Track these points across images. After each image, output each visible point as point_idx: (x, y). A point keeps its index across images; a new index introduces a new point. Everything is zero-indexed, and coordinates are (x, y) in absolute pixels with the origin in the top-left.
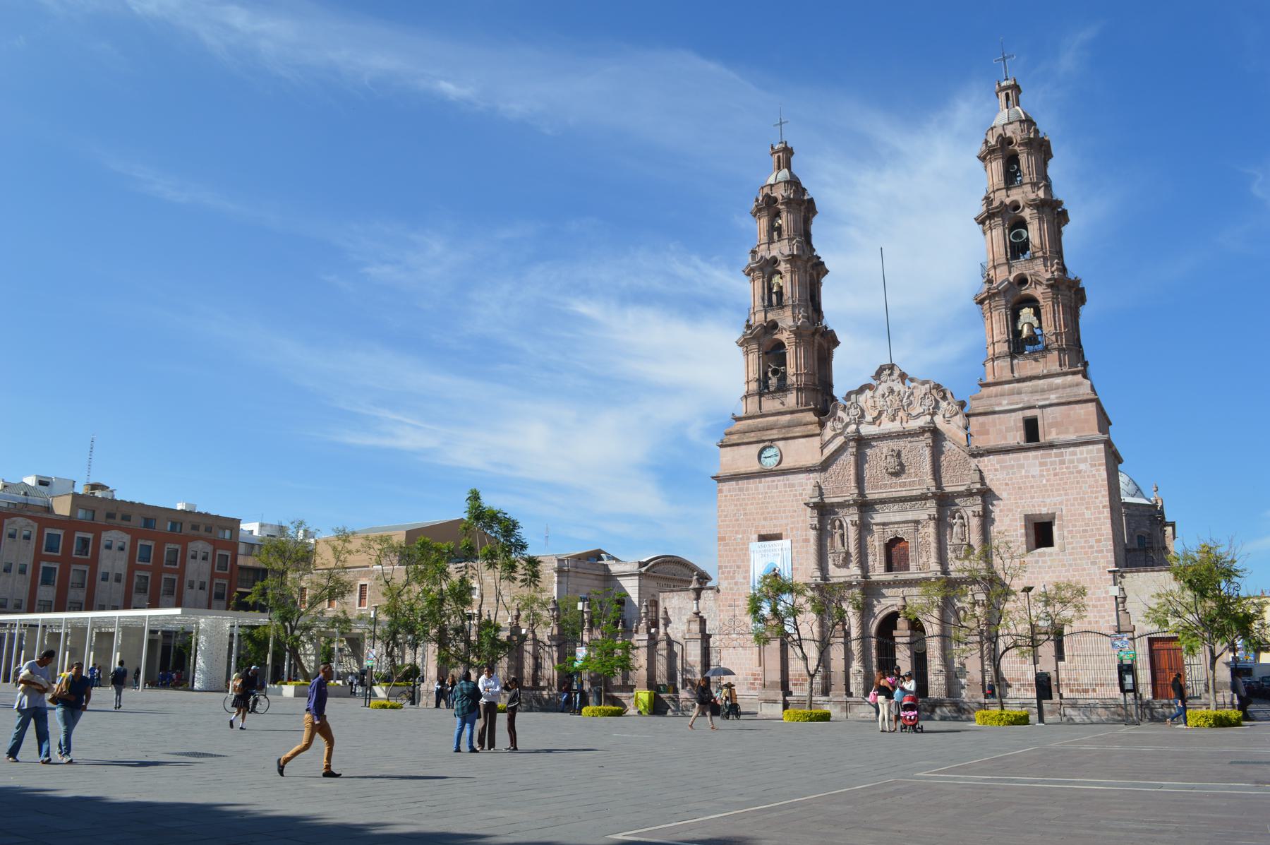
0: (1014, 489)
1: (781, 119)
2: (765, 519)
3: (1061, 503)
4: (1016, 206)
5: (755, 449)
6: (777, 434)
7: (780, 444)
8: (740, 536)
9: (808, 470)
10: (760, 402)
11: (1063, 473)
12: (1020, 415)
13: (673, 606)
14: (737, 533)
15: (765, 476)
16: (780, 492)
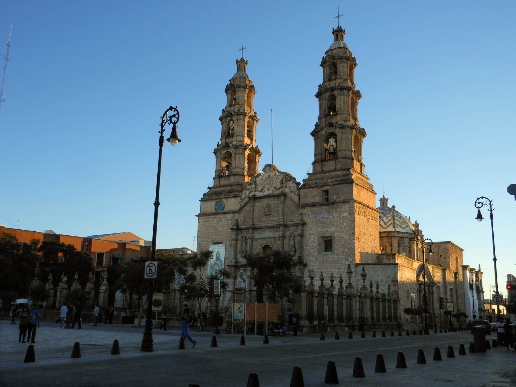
0: (316, 223)
1: (243, 47)
2: (216, 235)
3: (335, 231)
4: (332, 89)
5: (213, 203)
6: (224, 196)
7: (224, 200)
8: (206, 243)
9: (234, 212)
10: (219, 180)
11: (337, 217)
12: (321, 189)
14: (204, 241)
16: (223, 223)
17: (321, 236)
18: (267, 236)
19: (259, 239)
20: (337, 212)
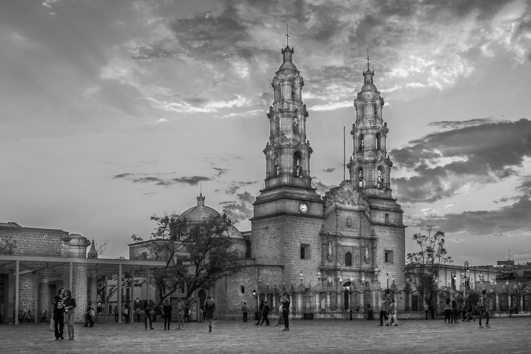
2: (303, 237)
8: (293, 243)
13: (263, 273)
14: (292, 241)
15: (304, 217)
17: (385, 250)
19: (342, 246)
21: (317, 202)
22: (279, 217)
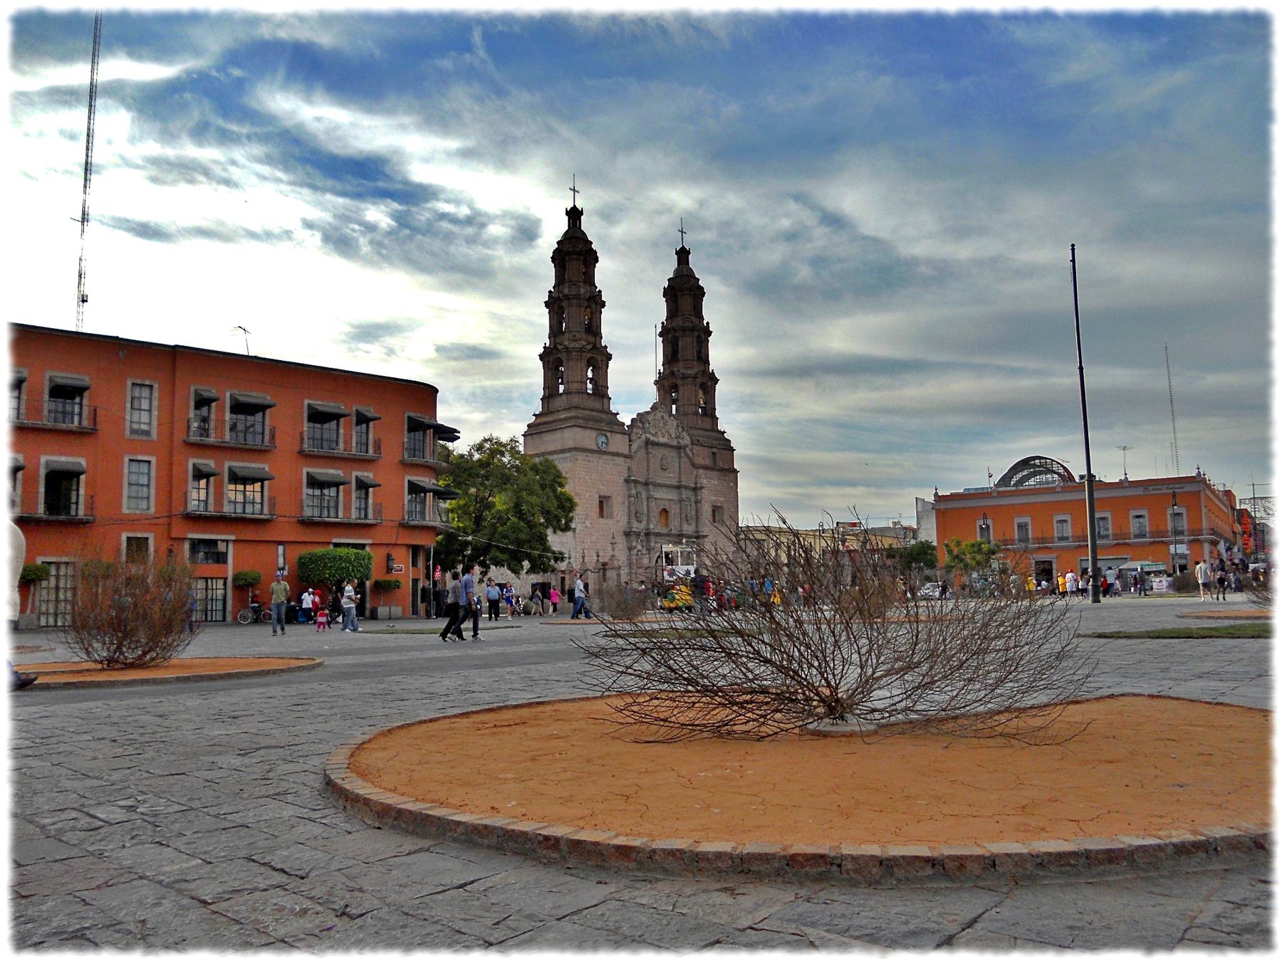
2: (603, 485)
5: (594, 434)
7: (609, 434)
8: (587, 495)
18: (665, 497)
20: (725, 480)
21: (621, 433)
22: (568, 455)
